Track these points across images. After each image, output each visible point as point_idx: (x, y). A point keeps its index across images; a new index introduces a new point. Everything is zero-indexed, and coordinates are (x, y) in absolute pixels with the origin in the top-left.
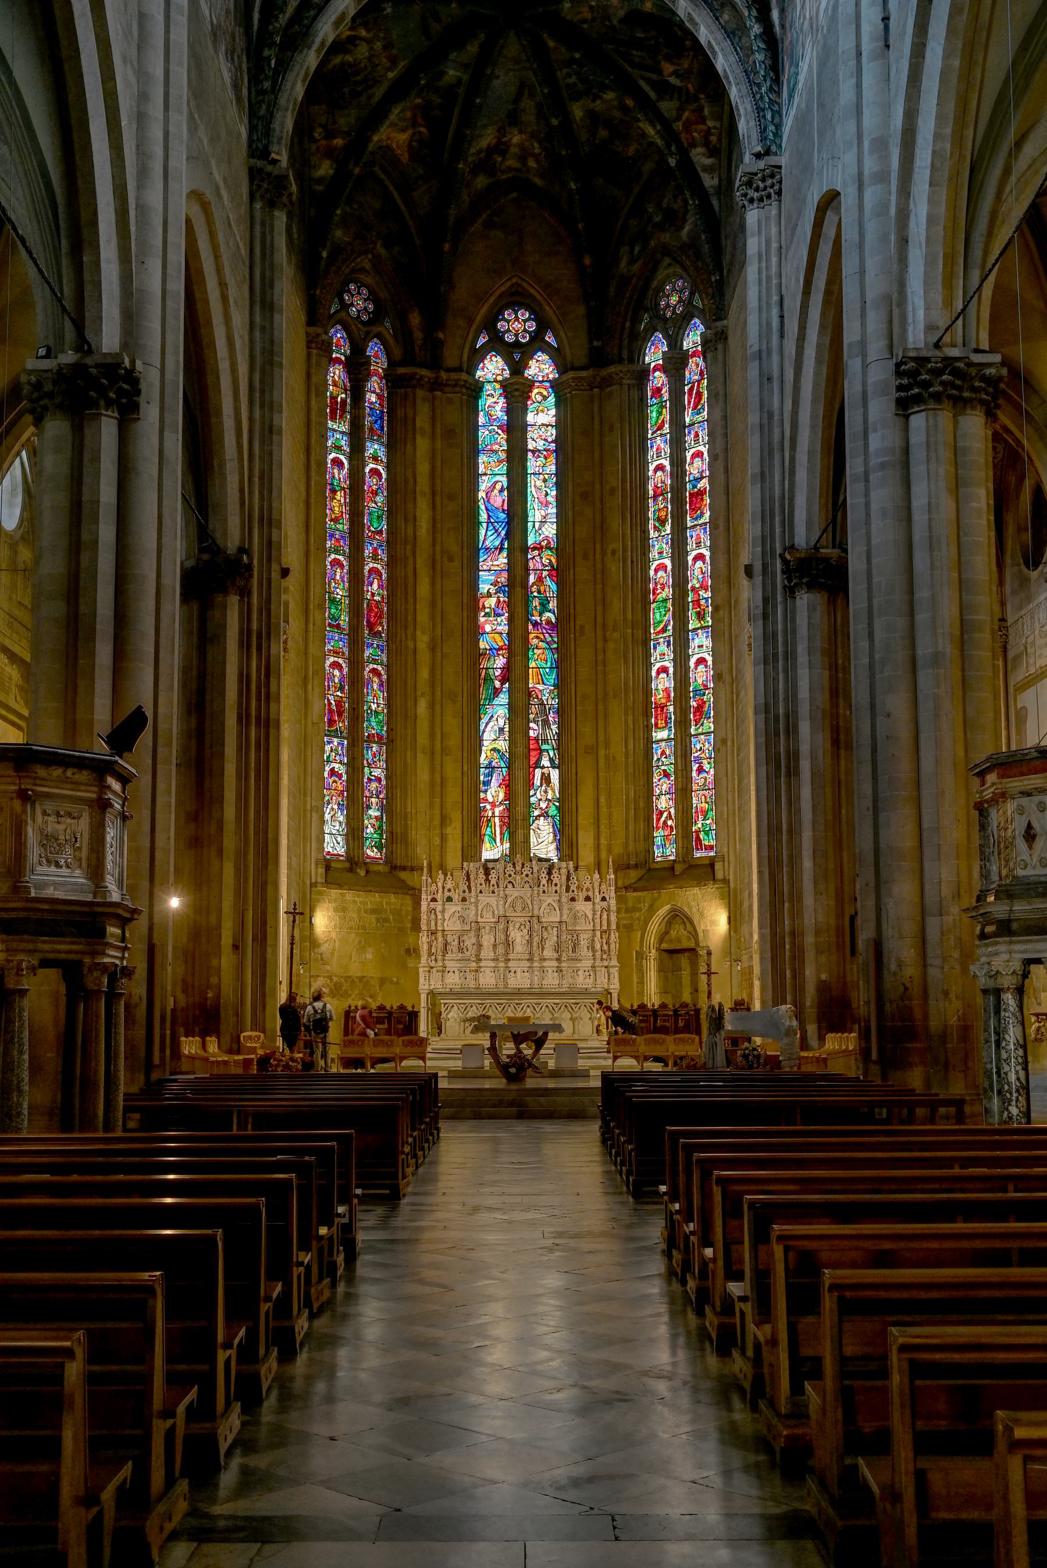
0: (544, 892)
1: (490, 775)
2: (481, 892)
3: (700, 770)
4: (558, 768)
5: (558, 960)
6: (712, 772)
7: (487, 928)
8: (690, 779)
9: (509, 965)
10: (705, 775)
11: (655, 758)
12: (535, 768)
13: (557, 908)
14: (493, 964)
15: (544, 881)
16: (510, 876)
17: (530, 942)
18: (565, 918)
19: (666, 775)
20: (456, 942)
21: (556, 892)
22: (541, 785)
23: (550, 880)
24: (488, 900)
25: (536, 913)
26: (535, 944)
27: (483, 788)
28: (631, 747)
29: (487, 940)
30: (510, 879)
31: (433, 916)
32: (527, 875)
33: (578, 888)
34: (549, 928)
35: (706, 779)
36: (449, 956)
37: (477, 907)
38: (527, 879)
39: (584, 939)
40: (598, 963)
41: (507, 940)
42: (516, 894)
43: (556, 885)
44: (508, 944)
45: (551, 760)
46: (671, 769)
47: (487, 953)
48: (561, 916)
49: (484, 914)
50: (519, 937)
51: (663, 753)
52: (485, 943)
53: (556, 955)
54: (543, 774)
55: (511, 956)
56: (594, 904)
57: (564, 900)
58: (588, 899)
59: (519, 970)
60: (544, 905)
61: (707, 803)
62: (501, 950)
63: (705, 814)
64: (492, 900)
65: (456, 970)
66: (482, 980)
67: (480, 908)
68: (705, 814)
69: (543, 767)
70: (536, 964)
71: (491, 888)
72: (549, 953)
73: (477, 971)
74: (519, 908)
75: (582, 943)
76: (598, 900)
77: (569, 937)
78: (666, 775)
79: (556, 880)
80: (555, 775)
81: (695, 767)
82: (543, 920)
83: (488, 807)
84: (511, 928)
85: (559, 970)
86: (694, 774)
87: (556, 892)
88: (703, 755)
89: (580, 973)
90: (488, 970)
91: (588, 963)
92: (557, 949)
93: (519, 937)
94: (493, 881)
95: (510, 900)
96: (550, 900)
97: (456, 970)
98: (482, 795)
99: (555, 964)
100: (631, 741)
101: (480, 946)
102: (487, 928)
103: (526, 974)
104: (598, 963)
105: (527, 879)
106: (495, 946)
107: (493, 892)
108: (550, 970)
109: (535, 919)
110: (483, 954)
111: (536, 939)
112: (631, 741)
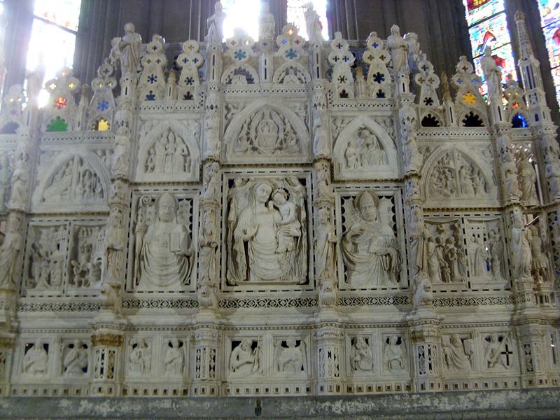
0: (344, 95)
2: (151, 97)
5: (401, 301)
7: (165, 199)
9: (239, 317)
11: (474, 45)
13: (387, 141)
14: (173, 317)
15: (342, 69)
17: (304, 243)
18: (415, 163)
20: (63, 253)
21: (381, 95)
23: (359, 66)
25: (321, 150)
26: (322, 248)
28: (438, 32)
29: (163, 237)
30: (239, 63)
32: (291, 54)
33: (440, 92)
34: (368, 200)
36: (41, 293)
37: (135, 141)
38: (290, 62)
39: (476, 237)
40: (531, 308)
41: (229, 241)
42: (258, 103)
43: (379, 78)
44: (233, 251)
47: (159, 281)
48: (402, 160)
49: (158, 160)
50: (267, 228)
51: (488, 34)
52: (155, 251)
55: (241, 292)
56: (495, 132)
57: (409, 111)
59: (266, 339)
60: (347, 133)
62: (208, 268)
64: (183, 122)
65: (52, 339)
66: (133, 376)
67: (145, 142)
70: (327, 314)
71: (183, 88)
72: (367, 279)
73: (117, 341)
74: (268, 137)
75: (471, 247)
76: (505, 122)
77: (430, 232)
79: (376, 66)
82: (346, 174)
84: (240, 202)
85: (408, 335)
87: (381, 95)
89: (477, 344)
90: (159, 340)
91: (499, 313)
92: (393, 266)
93: (267, 228)
94: (189, 70)
95: (238, 119)
96: (362, 119)
97: (52, 339)
99: (392, 314)
100: (437, 24)
101: (137, 258)
102: (165, 199)
103: (293, 352)
104: (531, 308)
105: (290, 62)
106: (187, 259)
107: (188, 97)
108: (377, 336)
109: (321, 172)
110: (147, 288)
111: (325, 234)
112: (437, 24)
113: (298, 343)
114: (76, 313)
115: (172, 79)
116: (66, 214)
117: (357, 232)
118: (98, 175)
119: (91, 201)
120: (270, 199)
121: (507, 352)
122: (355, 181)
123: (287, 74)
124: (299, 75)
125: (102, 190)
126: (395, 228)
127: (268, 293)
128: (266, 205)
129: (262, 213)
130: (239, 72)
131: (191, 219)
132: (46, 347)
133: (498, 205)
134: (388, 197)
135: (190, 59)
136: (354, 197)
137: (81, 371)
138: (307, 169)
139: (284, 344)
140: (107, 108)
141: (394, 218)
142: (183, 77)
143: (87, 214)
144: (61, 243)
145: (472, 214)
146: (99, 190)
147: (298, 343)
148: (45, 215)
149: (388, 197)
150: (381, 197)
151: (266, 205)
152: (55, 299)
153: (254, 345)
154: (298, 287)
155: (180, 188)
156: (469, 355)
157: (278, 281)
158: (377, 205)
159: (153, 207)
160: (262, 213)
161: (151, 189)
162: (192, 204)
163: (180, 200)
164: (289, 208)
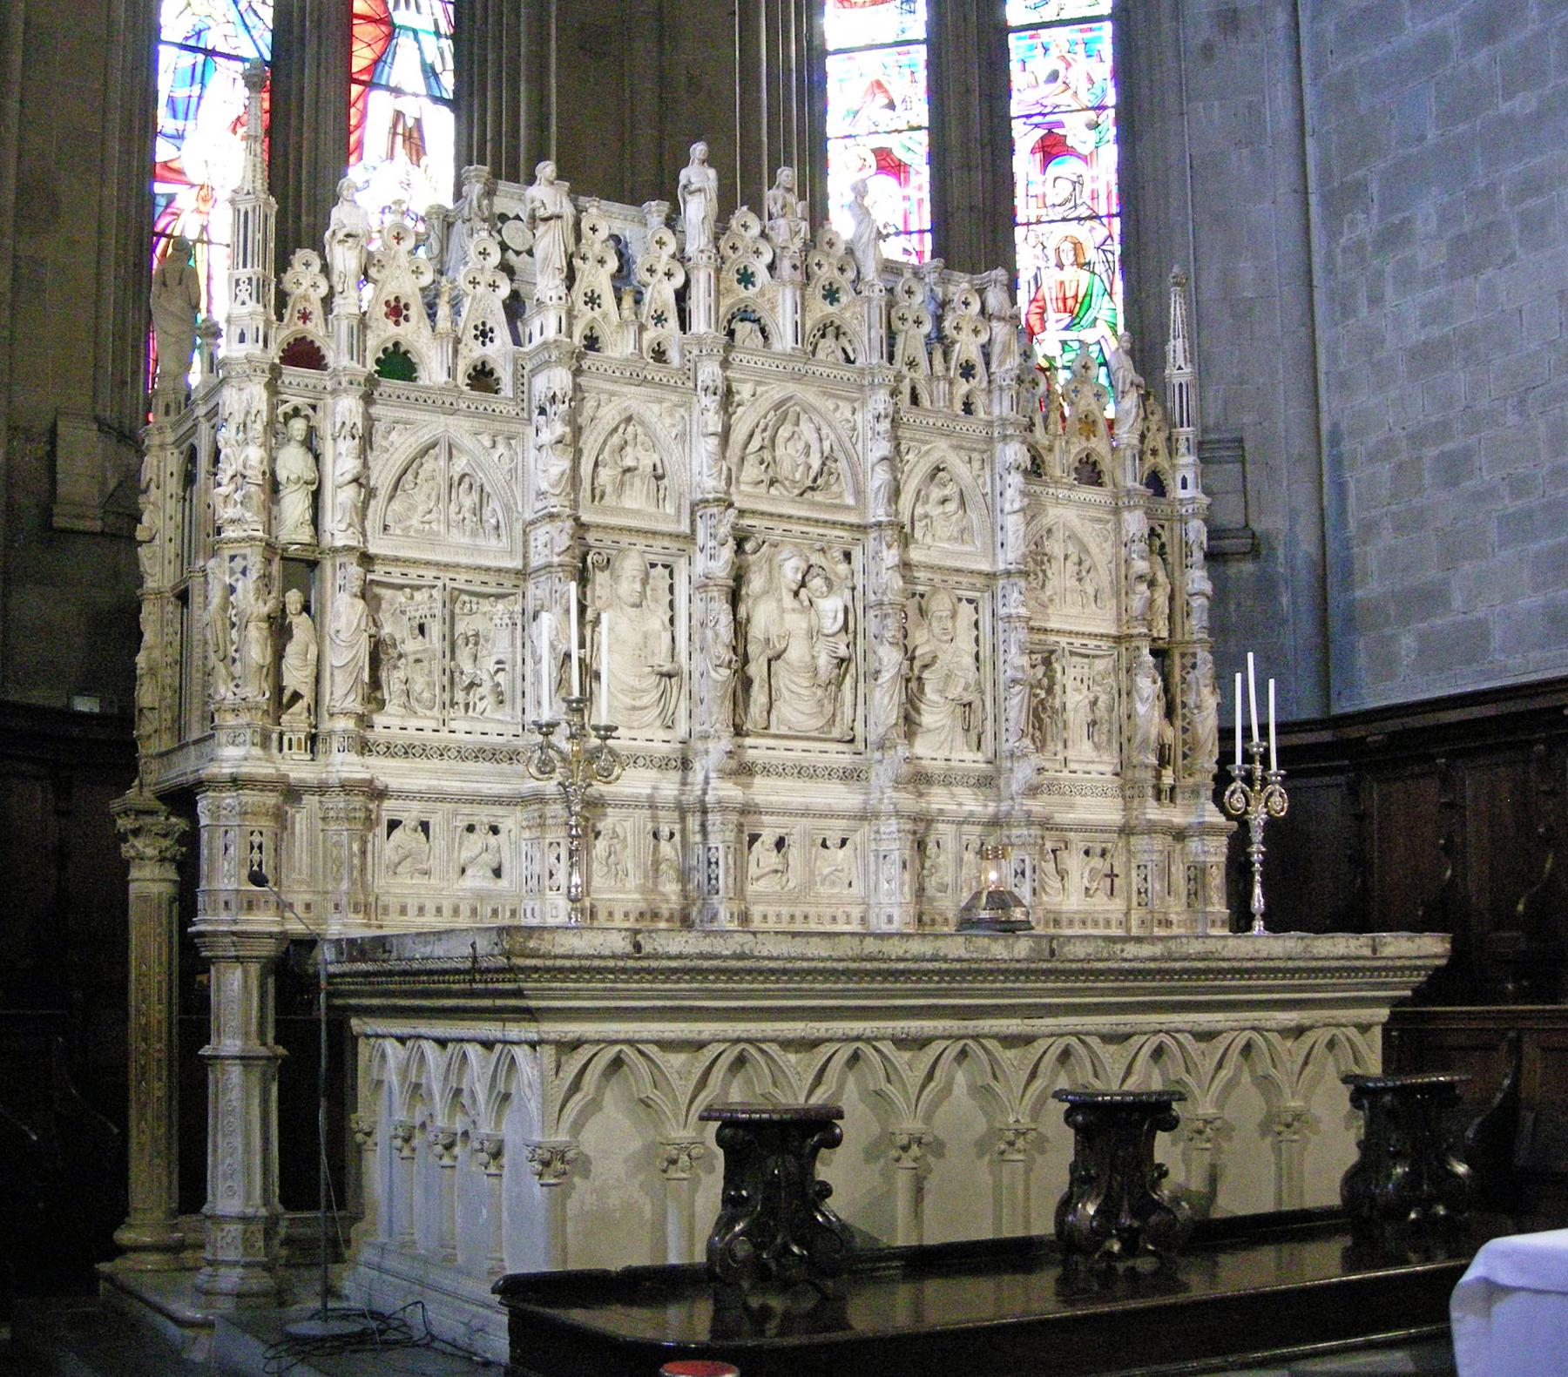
1: (198, 78)
3: (1051, 148)
4: (453, 104)
5: (986, 783)
6: (1110, 155)
8: (1003, 184)
10: (1064, 167)
12: (370, 85)
16: (746, 278)
19: (889, 164)
22: (391, 156)
24: (633, 399)
27: (164, 120)
31: (293, 462)
32: (831, 295)
34: (940, 605)
35: (1077, 183)
43: (967, 371)
45: (430, 72)
46: (915, 151)
53: (971, 760)
54: (399, 115)
55: (757, 749)
58: (1089, 472)
61: (1086, 265)
63: (1075, 309)
68: (1075, 309)
69: (397, 91)
78: (889, 164)
79: (967, 347)
80: (441, 128)
81: (1025, 138)
83: (185, 198)
86: (1024, 163)
88: (1065, 100)
89: (1074, 862)
98: (163, 151)
113: (844, 842)
114: (470, 765)
115: (628, 301)
116: (437, 564)
117: (927, 660)
118: (487, 488)
119: (480, 541)
120: (803, 584)
121: (1112, 876)
122: (931, 568)
123: (823, 336)
124: (844, 341)
125: (497, 527)
126: (977, 658)
127: (797, 752)
128: (796, 594)
129: (794, 610)
130: (745, 315)
131: (671, 605)
132: (425, 827)
133: (1113, 631)
134: (970, 601)
135: (661, 268)
136: (922, 596)
137: (490, 874)
138: (858, 536)
139: (824, 845)
140: (491, 340)
141: (977, 640)
142: (646, 310)
143: (478, 568)
144: (428, 621)
145: (1078, 642)
146: (493, 521)
147: (844, 842)
148: (397, 559)
149: (970, 601)
150: (960, 600)
151: (796, 594)
152: (428, 734)
153: (780, 844)
154: (842, 747)
155: (658, 544)
156: (1062, 874)
157: (816, 734)
158: (954, 615)
159: (607, 573)
160: (794, 610)
161: (608, 540)
162: (671, 575)
163: (653, 565)
164: (831, 607)
